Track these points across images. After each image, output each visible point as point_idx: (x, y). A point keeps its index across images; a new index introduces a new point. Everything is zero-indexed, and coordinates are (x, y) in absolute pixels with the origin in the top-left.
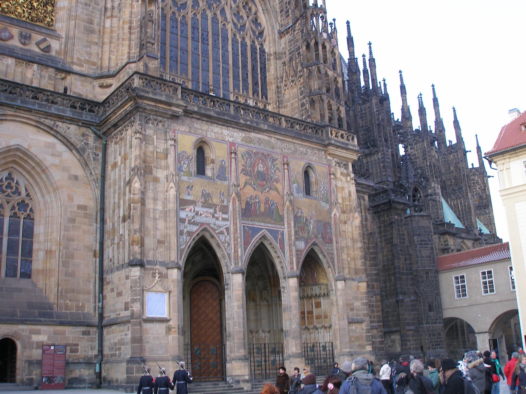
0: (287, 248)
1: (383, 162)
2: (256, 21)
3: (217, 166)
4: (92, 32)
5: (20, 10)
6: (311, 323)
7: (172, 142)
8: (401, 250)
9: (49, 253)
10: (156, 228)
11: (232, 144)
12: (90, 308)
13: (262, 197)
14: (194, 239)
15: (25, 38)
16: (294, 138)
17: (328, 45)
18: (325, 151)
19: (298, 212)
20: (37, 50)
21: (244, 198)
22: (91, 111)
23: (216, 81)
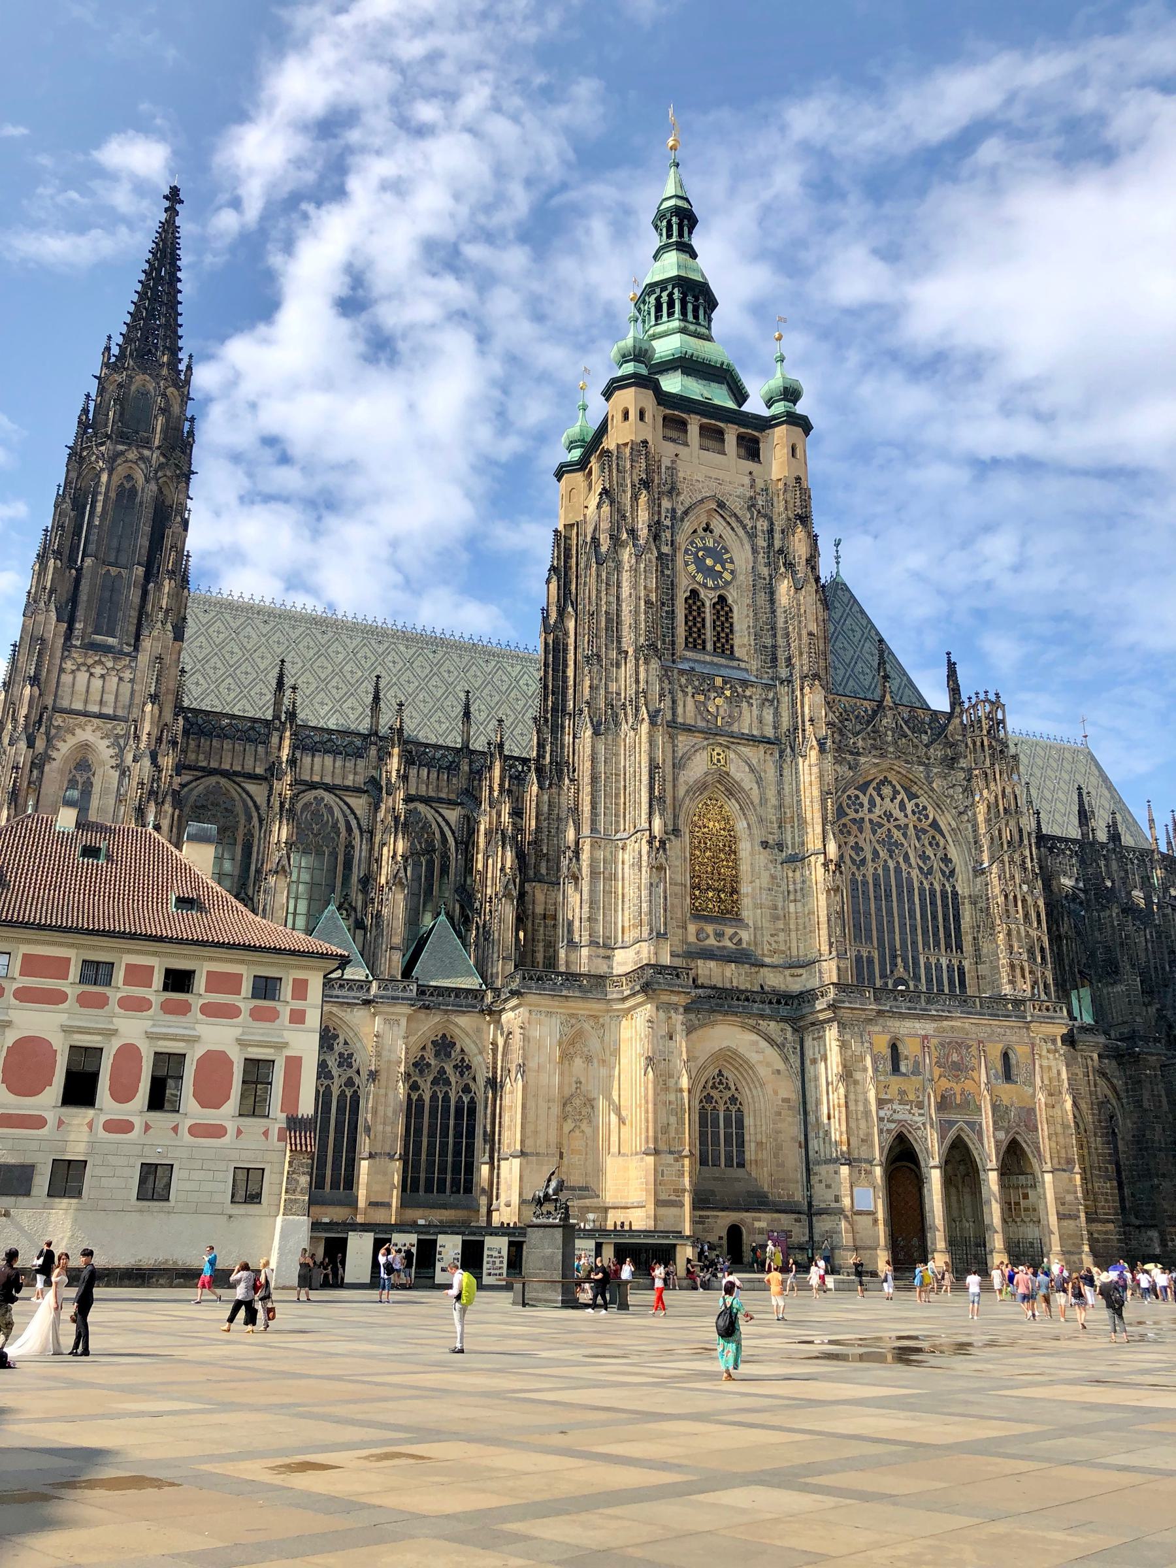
1: (1128, 996)
2: (946, 860)
3: (911, 1062)
4: (778, 918)
5: (711, 906)
6: (1019, 1216)
8: (1156, 1117)
9: (760, 1144)
10: (858, 1128)
11: (925, 1037)
12: (799, 1196)
13: (957, 1088)
15: (719, 935)
17: (1029, 899)
18: (1028, 1028)
20: (729, 944)
21: (939, 1093)
22: (786, 1004)
23: (903, 942)
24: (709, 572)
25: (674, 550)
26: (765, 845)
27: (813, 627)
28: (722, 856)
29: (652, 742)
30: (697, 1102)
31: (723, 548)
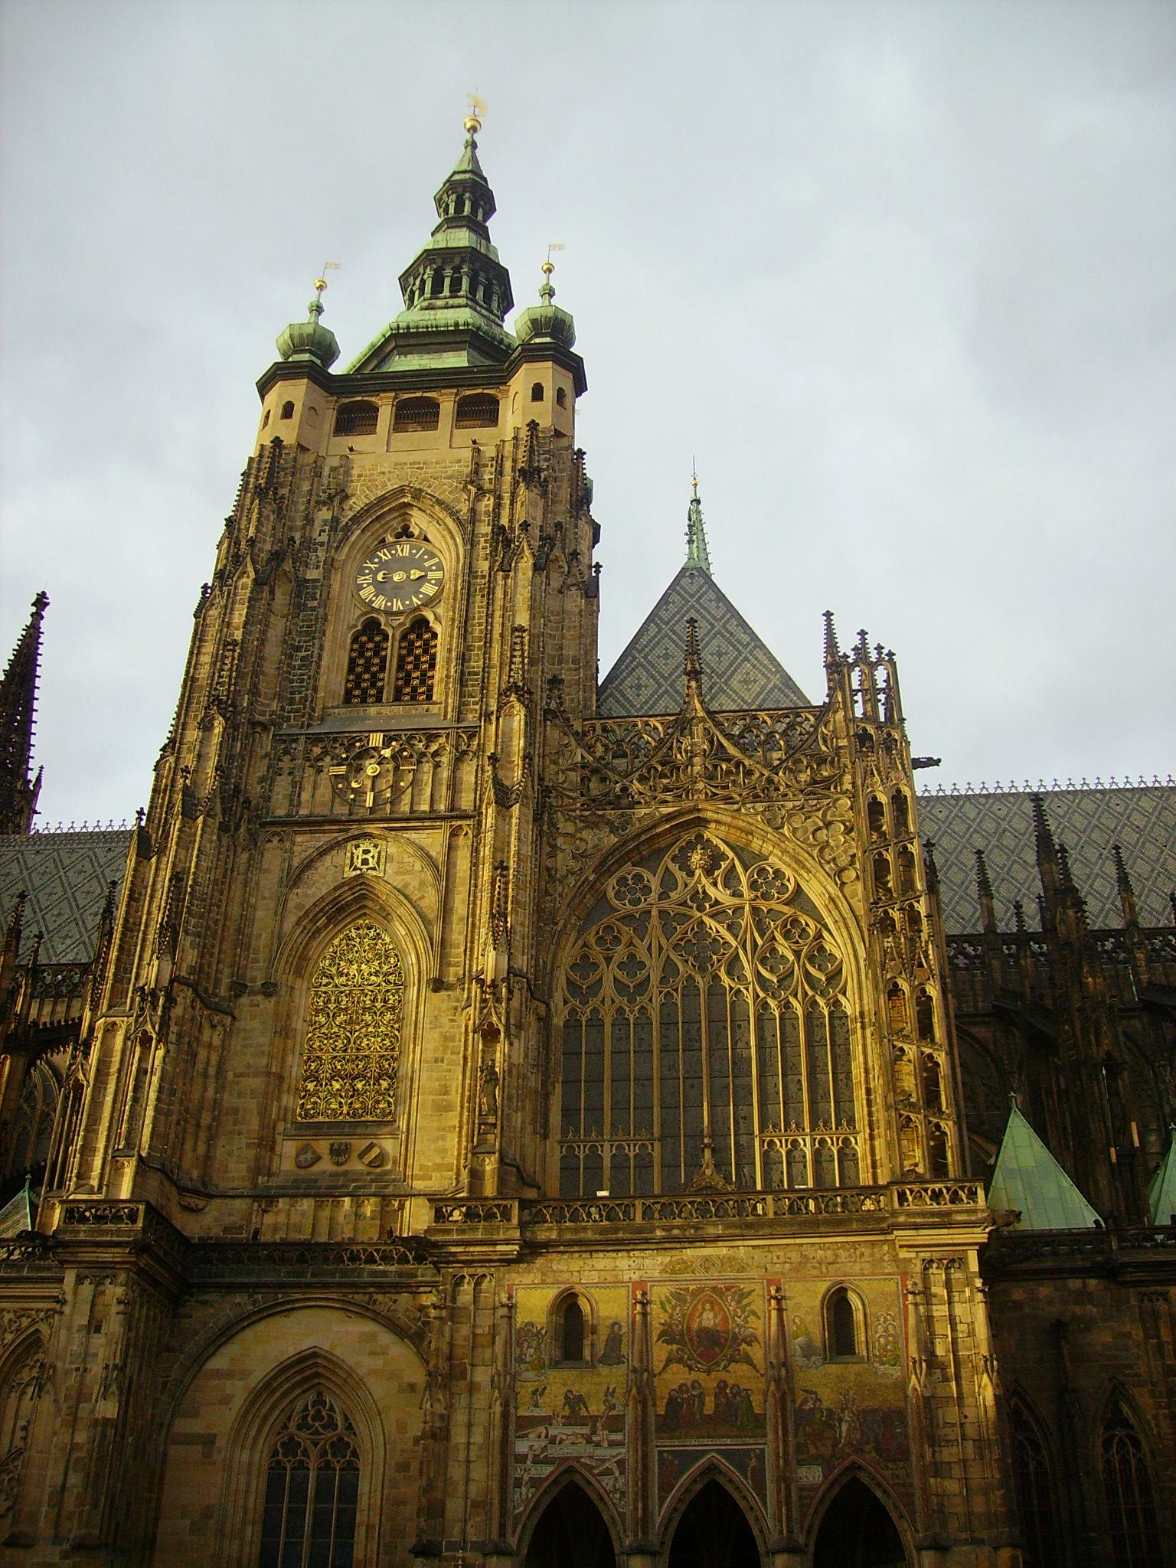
0: (770, 1486)
2: (819, 954)
3: (603, 1337)
4: (447, 1108)
7: (504, 1311)
10: (468, 1480)
11: (640, 1284)
13: (709, 1382)
14: (545, 1492)
15: (339, 1153)
16: (793, 1236)
17: (904, 985)
19: (805, 1401)
24: (397, 591)
25: (327, 576)
26: (438, 985)
27: (523, 619)
28: (368, 1018)
29: (184, 843)
30: (252, 1458)
31: (426, 552)
